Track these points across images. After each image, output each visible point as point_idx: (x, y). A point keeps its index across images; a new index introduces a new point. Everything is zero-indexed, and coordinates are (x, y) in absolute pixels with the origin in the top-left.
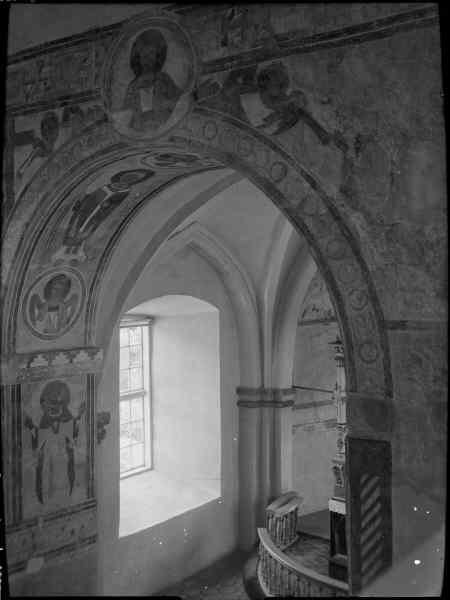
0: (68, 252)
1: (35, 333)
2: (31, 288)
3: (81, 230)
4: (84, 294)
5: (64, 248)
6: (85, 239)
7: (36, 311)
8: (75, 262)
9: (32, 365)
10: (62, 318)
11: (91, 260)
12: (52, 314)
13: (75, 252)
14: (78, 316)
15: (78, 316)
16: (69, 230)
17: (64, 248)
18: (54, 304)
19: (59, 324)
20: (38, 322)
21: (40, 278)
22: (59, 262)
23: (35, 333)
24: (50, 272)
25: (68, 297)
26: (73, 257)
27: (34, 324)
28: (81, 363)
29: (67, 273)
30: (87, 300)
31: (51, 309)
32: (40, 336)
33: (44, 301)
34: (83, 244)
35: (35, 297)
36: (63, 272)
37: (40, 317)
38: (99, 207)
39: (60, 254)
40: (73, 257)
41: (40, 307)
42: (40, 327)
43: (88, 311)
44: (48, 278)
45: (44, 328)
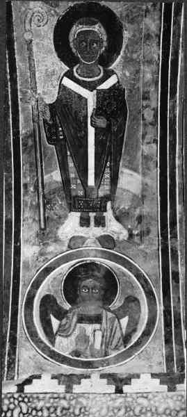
0: (85, 222)
1: (54, 355)
2: (36, 285)
3: (91, 181)
4: (150, 294)
5: (75, 217)
6: (107, 198)
7: (55, 323)
8: (107, 241)
9: (27, 389)
10: (112, 336)
11: (141, 235)
12: (89, 328)
13: (100, 222)
14: (147, 334)
15: (147, 334)
16: (66, 182)
17: (75, 217)
18: (92, 309)
19: (106, 343)
20: (58, 339)
21: (48, 271)
22: (75, 241)
23: (54, 355)
24: (66, 259)
25: (117, 303)
26: (95, 232)
27: (53, 343)
28: (145, 396)
29: (99, 260)
30: (160, 308)
31: (81, 320)
32: (64, 360)
33: (67, 306)
34: (109, 204)
35: (48, 301)
36: (89, 259)
37: (64, 331)
38: (91, 131)
39: (71, 225)
40: (99, 232)
41: (61, 314)
42: (64, 345)
43: (167, 324)
44: (65, 268)
45: (72, 348)
